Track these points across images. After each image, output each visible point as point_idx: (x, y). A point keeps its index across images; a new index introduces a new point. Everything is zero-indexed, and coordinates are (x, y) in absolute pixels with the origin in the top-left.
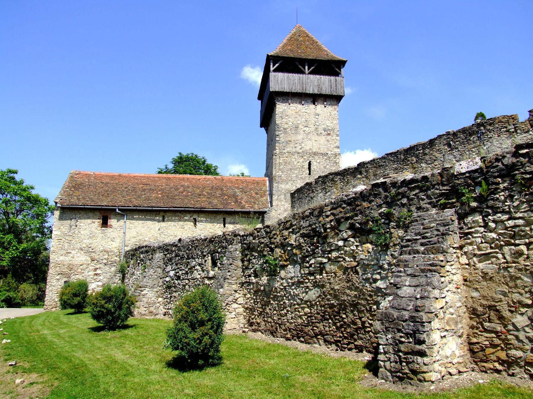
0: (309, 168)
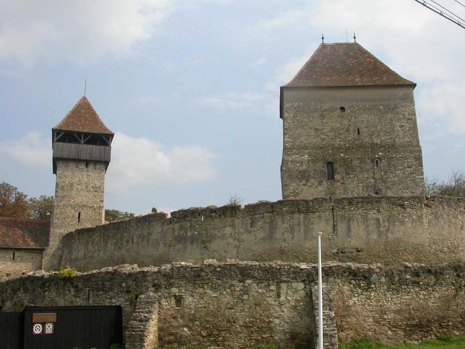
0: (79, 217)
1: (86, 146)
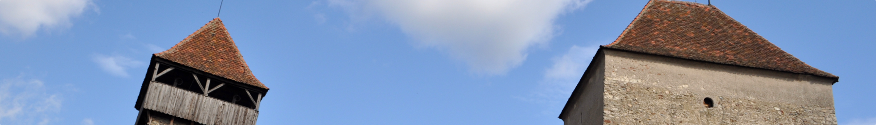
1: (211, 100)
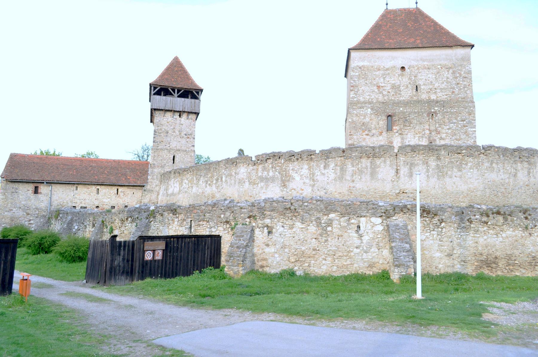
1: (179, 99)
